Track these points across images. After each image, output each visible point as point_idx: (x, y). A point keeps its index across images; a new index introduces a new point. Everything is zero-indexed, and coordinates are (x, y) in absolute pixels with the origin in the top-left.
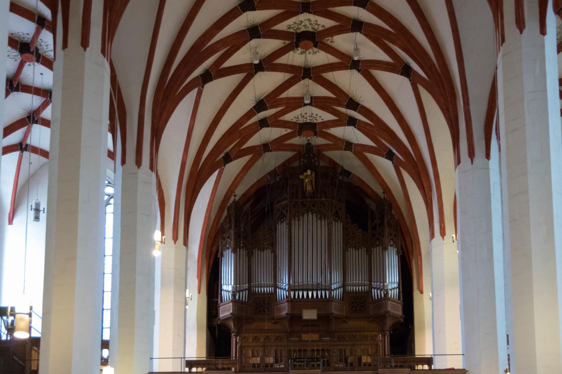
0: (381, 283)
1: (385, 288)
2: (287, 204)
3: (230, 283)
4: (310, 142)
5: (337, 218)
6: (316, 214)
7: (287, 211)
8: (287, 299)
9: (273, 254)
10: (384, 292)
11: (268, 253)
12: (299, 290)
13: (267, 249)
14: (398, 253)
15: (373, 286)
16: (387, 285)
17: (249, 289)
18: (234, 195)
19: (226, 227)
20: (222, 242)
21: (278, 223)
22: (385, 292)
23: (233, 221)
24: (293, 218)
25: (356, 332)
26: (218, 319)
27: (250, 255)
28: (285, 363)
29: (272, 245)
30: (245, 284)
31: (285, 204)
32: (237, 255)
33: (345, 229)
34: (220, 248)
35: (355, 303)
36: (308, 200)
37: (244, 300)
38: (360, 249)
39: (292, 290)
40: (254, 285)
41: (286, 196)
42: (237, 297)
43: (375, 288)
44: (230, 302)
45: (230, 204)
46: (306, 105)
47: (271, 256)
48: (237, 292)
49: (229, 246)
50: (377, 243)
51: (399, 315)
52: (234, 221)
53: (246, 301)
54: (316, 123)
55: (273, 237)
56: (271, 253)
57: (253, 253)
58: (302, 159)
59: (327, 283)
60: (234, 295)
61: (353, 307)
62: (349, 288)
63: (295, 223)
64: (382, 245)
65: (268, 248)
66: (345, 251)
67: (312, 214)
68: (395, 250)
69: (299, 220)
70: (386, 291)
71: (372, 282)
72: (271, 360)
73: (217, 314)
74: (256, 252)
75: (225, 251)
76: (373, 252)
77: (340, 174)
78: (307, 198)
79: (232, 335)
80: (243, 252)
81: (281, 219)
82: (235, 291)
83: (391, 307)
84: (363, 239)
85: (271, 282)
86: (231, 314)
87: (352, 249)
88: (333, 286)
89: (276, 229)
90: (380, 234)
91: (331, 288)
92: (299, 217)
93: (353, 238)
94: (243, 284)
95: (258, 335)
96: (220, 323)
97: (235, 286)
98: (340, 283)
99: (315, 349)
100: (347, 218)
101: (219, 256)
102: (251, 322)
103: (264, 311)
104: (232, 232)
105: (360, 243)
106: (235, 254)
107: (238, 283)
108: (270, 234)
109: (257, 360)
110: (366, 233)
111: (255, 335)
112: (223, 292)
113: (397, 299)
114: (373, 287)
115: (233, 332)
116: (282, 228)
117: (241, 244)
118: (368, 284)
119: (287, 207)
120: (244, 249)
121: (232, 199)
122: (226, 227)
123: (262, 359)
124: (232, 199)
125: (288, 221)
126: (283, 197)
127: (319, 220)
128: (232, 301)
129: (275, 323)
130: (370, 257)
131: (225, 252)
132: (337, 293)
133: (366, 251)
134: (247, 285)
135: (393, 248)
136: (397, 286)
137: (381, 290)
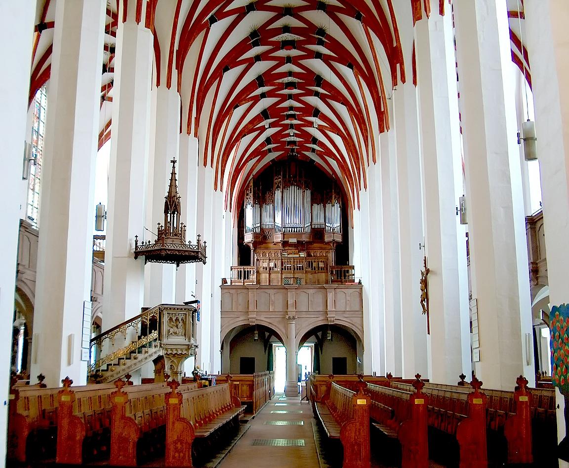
7: (281, 185)
17: (260, 226)
27: (261, 207)
63: (285, 191)
66: (312, 205)
69: (287, 190)
72: (272, 265)
74: (264, 205)
80: (258, 206)
101: (245, 207)
109: (266, 265)
116: (278, 194)
123: (269, 265)
124: (251, 176)
129: (275, 244)
132: (308, 230)
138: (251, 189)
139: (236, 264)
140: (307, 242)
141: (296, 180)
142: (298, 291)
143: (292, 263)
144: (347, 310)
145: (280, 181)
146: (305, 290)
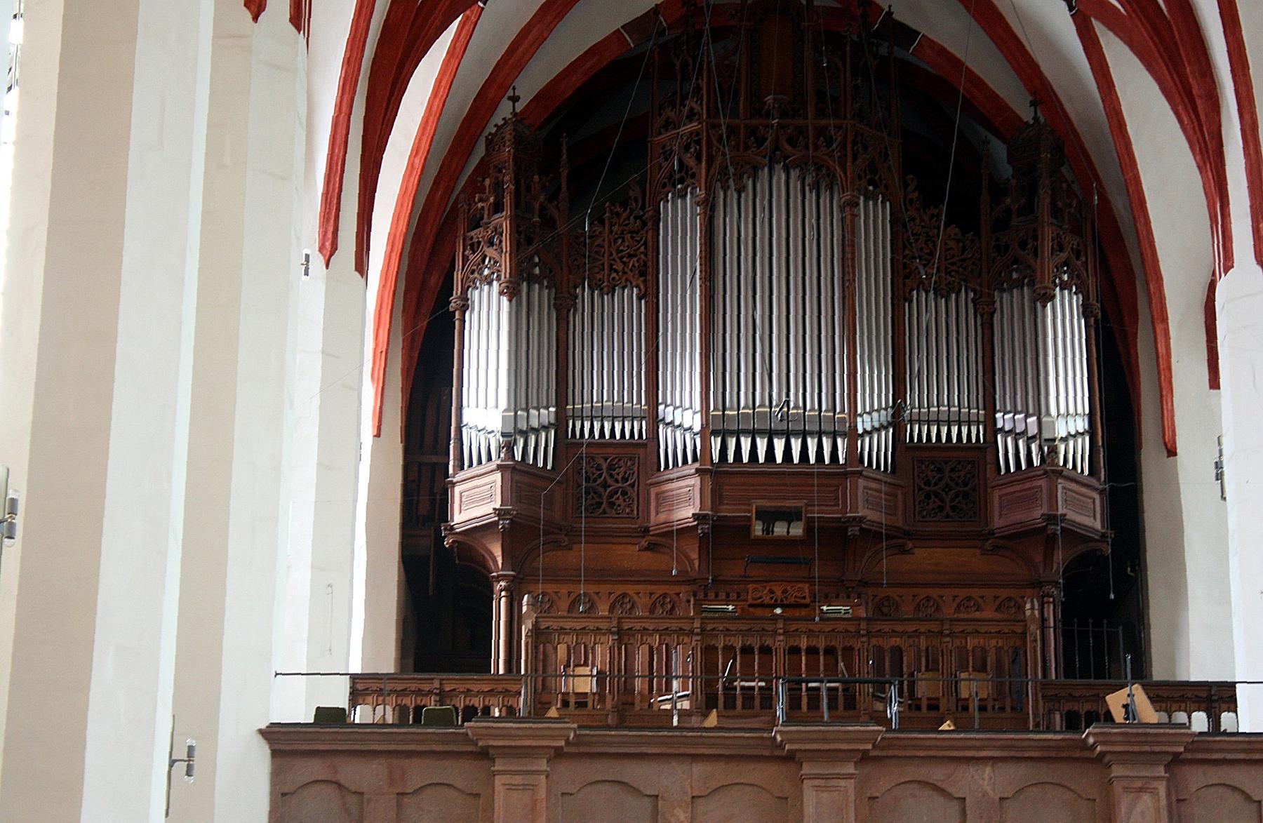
1: (1046, 435)
2: (698, 134)
3: (491, 402)
5: (871, 188)
6: (802, 169)
7: (699, 159)
8: (697, 465)
9: (646, 302)
10: (1041, 448)
11: (628, 300)
12: (738, 434)
13: (624, 288)
14: (1086, 311)
15: (1000, 425)
17: (560, 424)
18: (510, 98)
20: (465, 259)
22: (1046, 449)
23: (509, 186)
25: (944, 586)
26: (445, 529)
27: (564, 308)
28: (693, 693)
29: (643, 274)
30: (547, 408)
31: (691, 133)
32: (519, 304)
34: (458, 276)
35: (936, 484)
37: (540, 464)
39: (715, 433)
40: (578, 413)
41: (694, 105)
42: (518, 457)
45: (496, 125)
47: (639, 309)
48: (518, 437)
49: (493, 273)
50: (1015, 276)
51: (1094, 530)
52: (512, 187)
55: (645, 244)
56: (639, 299)
57: (576, 297)
60: (510, 448)
61: (928, 496)
62: (915, 432)
63: (727, 201)
64: (1032, 284)
65: (629, 285)
66: (900, 298)
70: (1050, 444)
76: (998, 305)
78: (768, 114)
80: (541, 296)
81: (674, 186)
83: (1066, 501)
84: (964, 260)
85: (639, 401)
88: (859, 419)
90: (1023, 245)
91: (856, 426)
92: (741, 178)
93: (930, 258)
96: (453, 541)
98: (883, 412)
99: (804, 644)
100: (906, 185)
103: (612, 505)
104: (503, 221)
105: (953, 273)
107: (524, 406)
108: (637, 233)
110: (972, 241)
112: (464, 430)
113: (1086, 472)
114: (1002, 429)
115: (498, 579)
117: (536, 265)
118: (982, 419)
119: (698, 142)
120: (545, 283)
121: (505, 110)
122: (483, 207)
124: (505, 110)
125: (701, 192)
127: (811, 191)
128: (499, 467)
129: (652, 547)
130: (988, 327)
131: (477, 292)
132: (878, 448)
133: (974, 301)
134: (552, 409)
136: (1087, 427)
137: (1030, 439)
138: (498, 187)
139: (387, 663)
140: (871, 535)
142: (884, 781)
143: (778, 662)
145: (695, 138)
146: (937, 774)
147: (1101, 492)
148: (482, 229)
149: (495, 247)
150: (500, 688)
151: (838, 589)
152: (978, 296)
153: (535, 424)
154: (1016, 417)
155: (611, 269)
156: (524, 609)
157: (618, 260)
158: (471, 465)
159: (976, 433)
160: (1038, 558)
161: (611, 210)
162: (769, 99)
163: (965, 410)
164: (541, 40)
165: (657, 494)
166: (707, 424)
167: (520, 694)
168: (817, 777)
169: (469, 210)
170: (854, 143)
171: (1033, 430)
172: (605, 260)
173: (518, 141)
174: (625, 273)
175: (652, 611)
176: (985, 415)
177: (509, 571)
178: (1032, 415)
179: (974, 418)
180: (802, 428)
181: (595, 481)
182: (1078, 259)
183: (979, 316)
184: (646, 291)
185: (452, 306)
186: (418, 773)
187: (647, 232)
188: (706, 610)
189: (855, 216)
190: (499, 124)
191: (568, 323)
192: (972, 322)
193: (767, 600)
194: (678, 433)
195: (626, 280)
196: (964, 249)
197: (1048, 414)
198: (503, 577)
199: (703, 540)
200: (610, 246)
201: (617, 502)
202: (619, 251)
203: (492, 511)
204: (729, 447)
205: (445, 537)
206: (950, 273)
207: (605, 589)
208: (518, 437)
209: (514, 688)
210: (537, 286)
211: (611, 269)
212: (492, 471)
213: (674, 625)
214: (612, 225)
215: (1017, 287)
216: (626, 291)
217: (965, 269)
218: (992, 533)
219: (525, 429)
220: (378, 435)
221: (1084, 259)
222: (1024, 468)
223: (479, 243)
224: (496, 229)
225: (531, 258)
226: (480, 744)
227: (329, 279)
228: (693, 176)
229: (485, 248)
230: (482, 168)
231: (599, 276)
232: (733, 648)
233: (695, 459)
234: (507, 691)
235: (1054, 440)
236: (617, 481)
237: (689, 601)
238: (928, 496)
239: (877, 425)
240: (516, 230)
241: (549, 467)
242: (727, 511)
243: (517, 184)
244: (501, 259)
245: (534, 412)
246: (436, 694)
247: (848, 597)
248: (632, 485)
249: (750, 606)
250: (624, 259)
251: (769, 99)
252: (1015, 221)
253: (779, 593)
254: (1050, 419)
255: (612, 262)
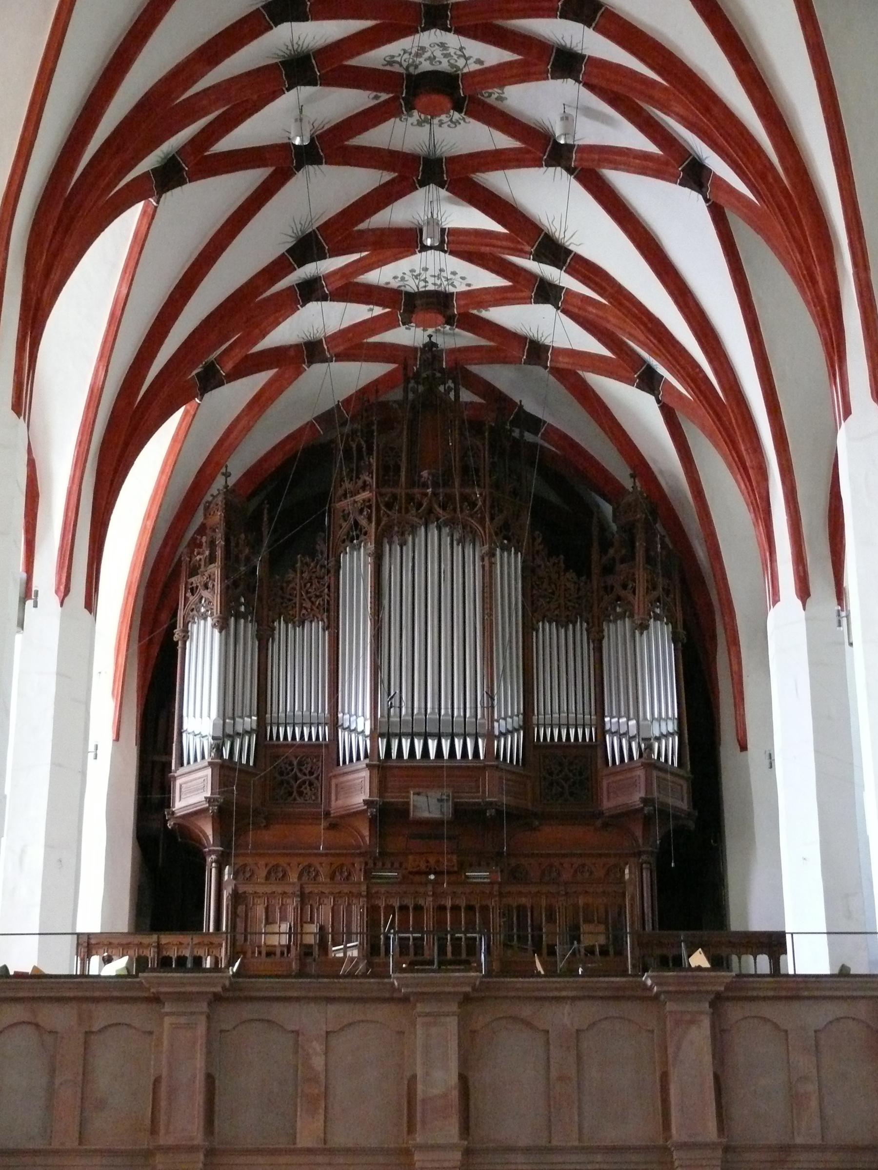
0: (629, 719)
2: (369, 500)
4: (433, 339)
5: (506, 542)
6: (451, 527)
7: (369, 519)
8: (367, 761)
13: (311, 622)
14: (675, 639)
15: (607, 727)
16: (649, 727)
18: (223, 474)
19: (198, 558)
20: (186, 599)
21: (346, 550)
22: (643, 746)
23: (220, 542)
24: (386, 540)
26: (168, 814)
27: (264, 638)
28: (360, 943)
30: (250, 717)
31: (364, 501)
33: (529, 572)
34: (181, 614)
35: (558, 775)
36: (428, 491)
37: (244, 761)
38: (571, 626)
39: (382, 735)
41: (367, 479)
42: (226, 755)
43: (613, 734)
44: (205, 767)
45: (212, 495)
46: (425, 248)
49: (208, 611)
50: (618, 610)
51: (682, 811)
52: (223, 543)
53: (251, 764)
54: (452, 294)
55: (329, 587)
56: (324, 630)
58: (412, 384)
59: (479, 717)
60: (219, 749)
61: (551, 784)
62: (541, 733)
64: (631, 616)
65: (316, 620)
66: (528, 629)
67: (439, 529)
68: (667, 630)
70: (646, 742)
71: (603, 716)
73: (166, 801)
74: (281, 626)
75: (195, 623)
76: (606, 633)
77: (515, 423)
78: (425, 485)
79: (209, 860)
80: (247, 629)
81: (352, 541)
82: (219, 734)
86: (208, 800)
87: (547, 625)
88: (496, 724)
89: (340, 567)
90: (625, 587)
91: (493, 727)
92: (403, 534)
94: (242, 717)
95: (283, 861)
96: (174, 824)
97: (222, 722)
98: (516, 718)
100: (534, 539)
101: (177, 635)
102: (263, 825)
103: (301, 794)
104: (216, 570)
106: (224, 632)
107: (230, 714)
111: (273, 862)
112: (184, 735)
113: (676, 764)
114: (610, 731)
115: (211, 852)
117: (241, 604)
118: (594, 722)
119: (370, 507)
120: (250, 618)
121: (219, 483)
122: (200, 560)
125: (371, 547)
126: (360, 483)
127: (458, 544)
128: (210, 764)
129: (333, 826)
130: (599, 650)
131: (195, 626)
133: (587, 630)
134: (255, 718)
135: (661, 624)
136: (676, 729)
138: (212, 544)
141: (449, 498)
144: (799, 1140)
145: (367, 503)
146: (526, 1011)
147: (687, 779)
148: (199, 576)
149: (209, 590)
150: (206, 940)
151: (481, 860)
152: (591, 624)
153: (240, 729)
154: (621, 721)
155: (302, 607)
156: (226, 877)
157: (307, 600)
158: (189, 763)
159: (590, 733)
160: (639, 833)
161: (302, 561)
162: (425, 473)
163: (580, 716)
164: (248, 429)
165: (337, 785)
166: (375, 728)
167: (221, 945)
168: (427, 1015)
169: (190, 562)
170: (492, 507)
171: (633, 731)
172: (297, 600)
173: (229, 507)
174: (312, 610)
175: (332, 878)
176: (597, 720)
177: (218, 846)
178: (632, 719)
179: (587, 721)
180: (451, 731)
181: (288, 774)
182: (668, 596)
183: (591, 641)
184: (329, 623)
185: (176, 638)
186: (103, 1015)
187: (330, 578)
188: (374, 877)
189: (492, 564)
190: (215, 494)
191: (267, 649)
192: (585, 648)
193: (423, 867)
194: (353, 735)
195: (314, 616)
196: (579, 589)
197: (645, 718)
198: (214, 852)
199: (372, 821)
200: (301, 588)
201: (305, 791)
202: (307, 592)
203: (204, 799)
204: (393, 747)
205: (168, 820)
206: (568, 608)
207: (294, 861)
208: (226, 740)
209: (215, 940)
210: (242, 621)
211: (302, 607)
212: (205, 767)
213: (346, 889)
214: (302, 572)
215: (620, 619)
216: (313, 624)
217: (580, 604)
218: (601, 814)
219: (232, 733)
220: (117, 738)
221: (672, 596)
222: (626, 761)
223: (197, 587)
224: (210, 576)
225: (239, 598)
226: (152, 990)
227: (63, 615)
228: (365, 534)
229: (201, 590)
230: (202, 530)
231: (291, 612)
232: (393, 907)
233: (366, 756)
234: (212, 943)
235: (650, 739)
236: (305, 774)
237: (361, 870)
238: (551, 784)
239: (510, 728)
240: (225, 576)
241: (251, 764)
242: (391, 798)
243: (227, 540)
244: (213, 598)
245: (238, 720)
246: (154, 947)
247: (488, 864)
248: (317, 778)
249: (410, 873)
250: (313, 599)
251: (425, 473)
252: (619, 567)
253: (432, 860)
254: (646, 722)
255: (303, 602)
